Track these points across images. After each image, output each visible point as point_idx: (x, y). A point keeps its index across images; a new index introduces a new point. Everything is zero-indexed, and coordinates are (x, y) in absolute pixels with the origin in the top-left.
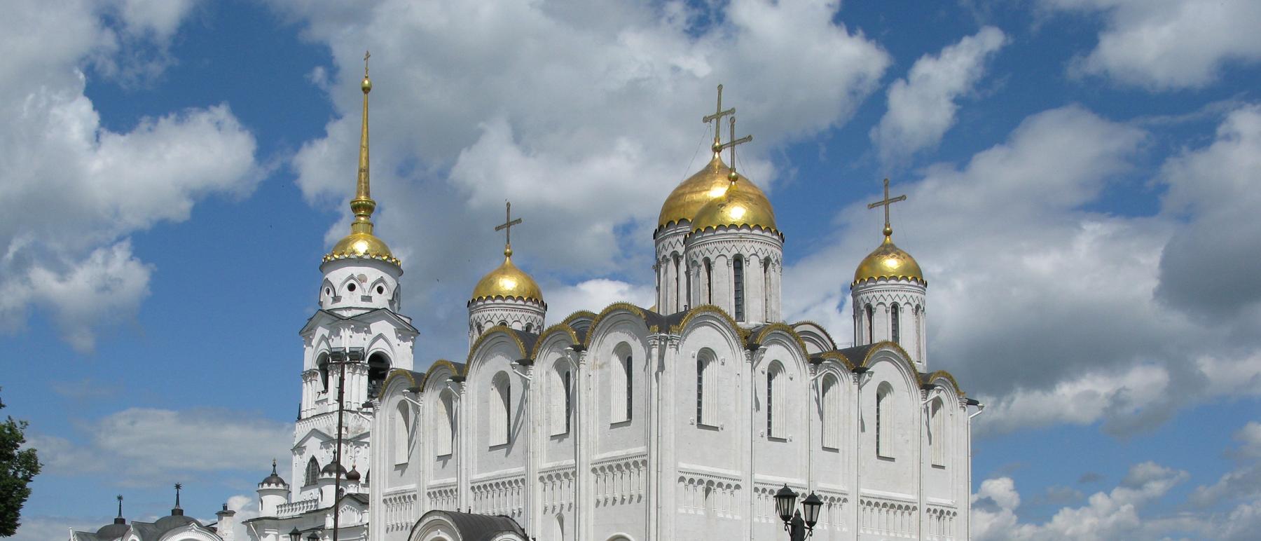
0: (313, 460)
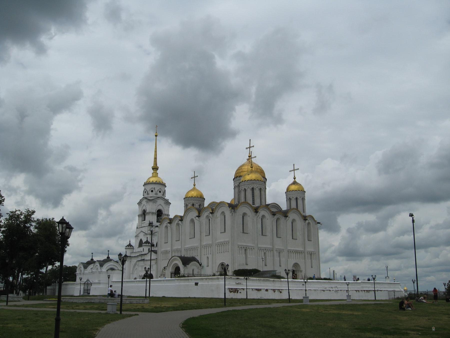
0: (141, 240)
